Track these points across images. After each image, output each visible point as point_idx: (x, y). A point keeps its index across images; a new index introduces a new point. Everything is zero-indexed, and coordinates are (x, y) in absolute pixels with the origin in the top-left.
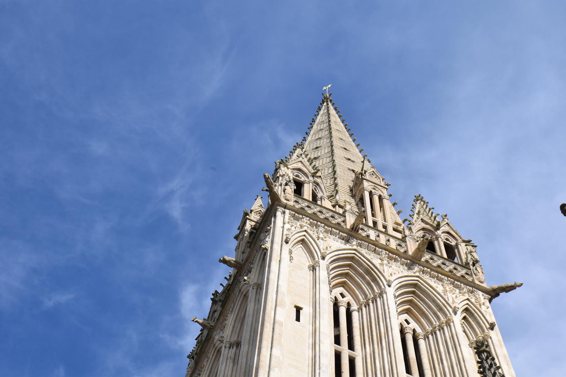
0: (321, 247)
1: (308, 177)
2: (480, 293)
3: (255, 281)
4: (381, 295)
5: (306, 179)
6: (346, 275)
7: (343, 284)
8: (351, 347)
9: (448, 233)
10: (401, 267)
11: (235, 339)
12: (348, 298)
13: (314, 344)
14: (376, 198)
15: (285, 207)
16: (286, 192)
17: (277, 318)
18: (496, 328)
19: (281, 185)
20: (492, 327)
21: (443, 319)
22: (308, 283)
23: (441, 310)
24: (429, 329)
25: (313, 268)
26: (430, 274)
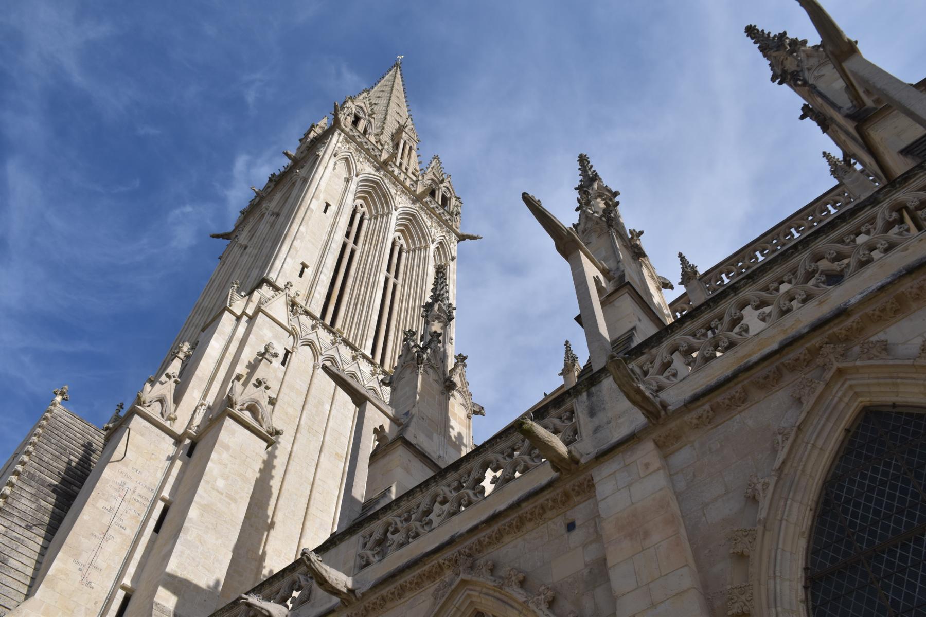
0: (358, 168)
1: (365, 116)
2: (454, 234)
3: (304, 176)
4: (388, 214)
6: (369, 193)
7: (364, 199)
8: (356, 242)
9: (447, 188)
11: (277, 211)
12: (365, 209)
13: (331, 232)
14: (408, 147)
15: (342, 130)
17: (311, 206)
18: (455, 260)
20: (453, 259)
22: (340, 191)
23: (424, 237)
24: (412, 247)
25: (347, 180)
26: (426, 211)
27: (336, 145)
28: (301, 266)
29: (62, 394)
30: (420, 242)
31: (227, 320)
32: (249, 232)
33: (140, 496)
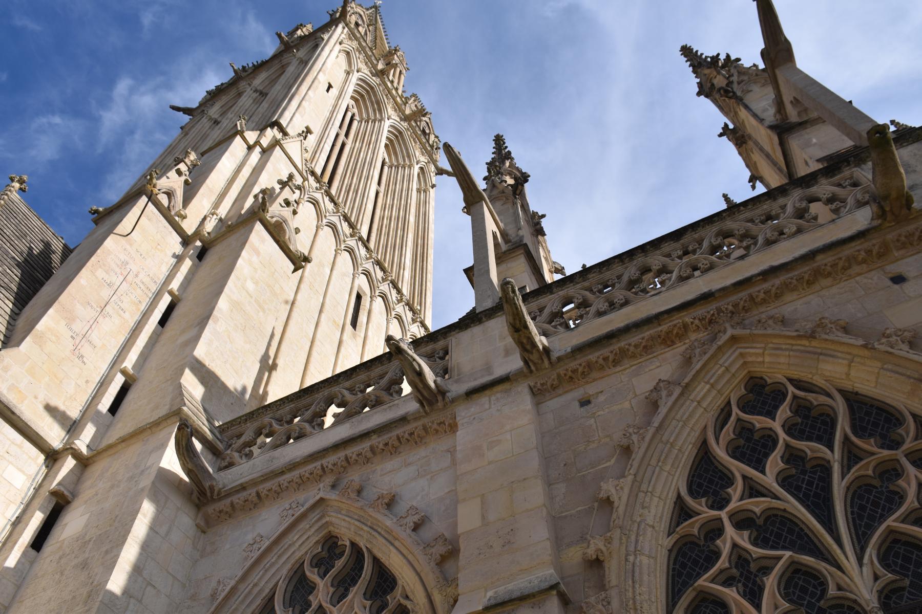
1: (364, 24)
3: (301, 56)
4: (380, 121)
6: (362, 96)
8: (347, 135)
9: (427, 123)
11: (261, 89)
12: (355, 110)
23: (409, 157)
25: (348, 73)
27: (340, 35)
29: (21, 182)
30: (404, 161)
31: (237, 147)
32: (221, 107)
33: (143, 283)
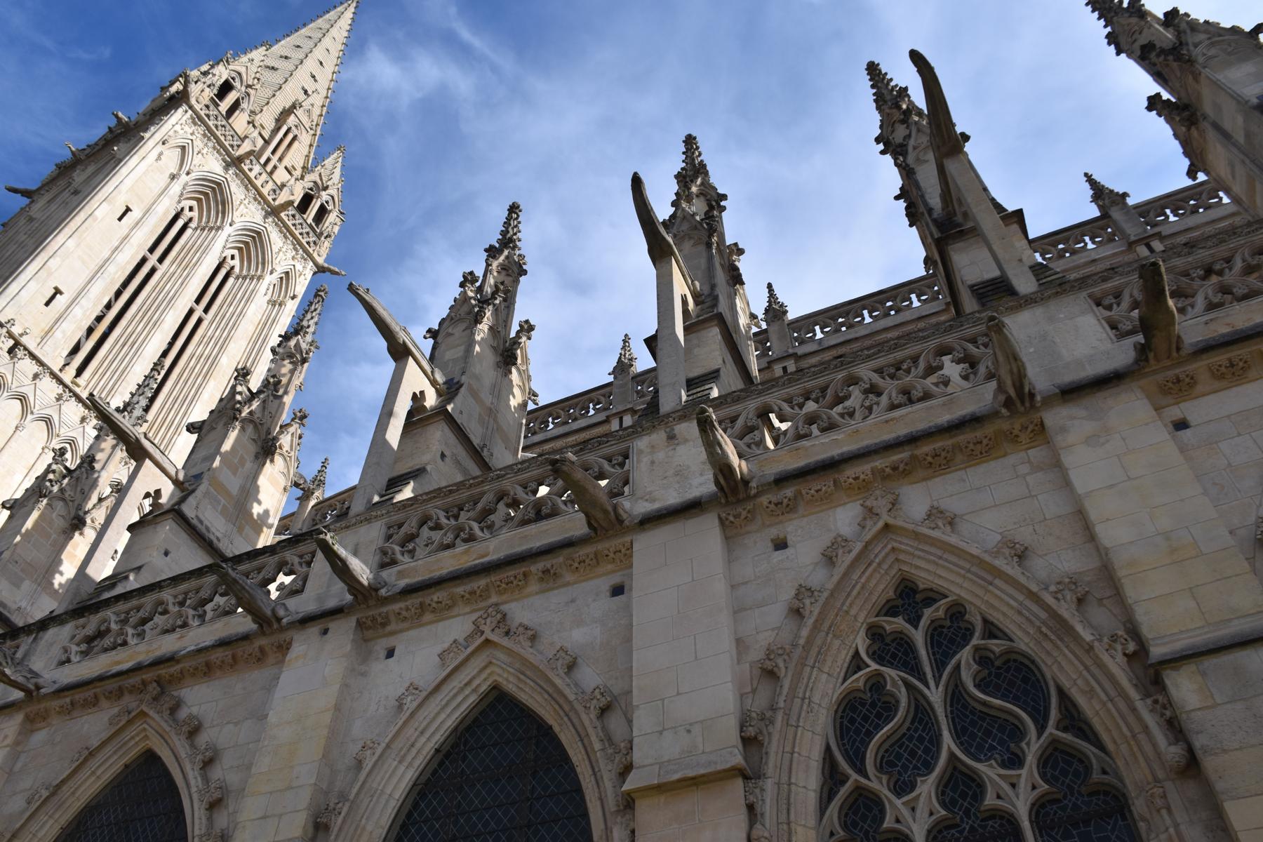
0: (193, 163)
2: (311, 264)
4: (219, 228)
5: (239, 87)
7: (199, 200)
9: (333, 197)
10: (260, 211)
12: (195, 214)
13: (117, 248)
14: (290, 137)
15: (191, 107)
16: (202, 94)
17: (96, 213)
19: (204, 83)
20: (293, 297)
21: (259, 273)
22: (157, 191)
23: (263, 264)
24: (245, 272)
25: (173, 177)
26: (281, 228)
27: (173, 126)
28: (54, 291)
